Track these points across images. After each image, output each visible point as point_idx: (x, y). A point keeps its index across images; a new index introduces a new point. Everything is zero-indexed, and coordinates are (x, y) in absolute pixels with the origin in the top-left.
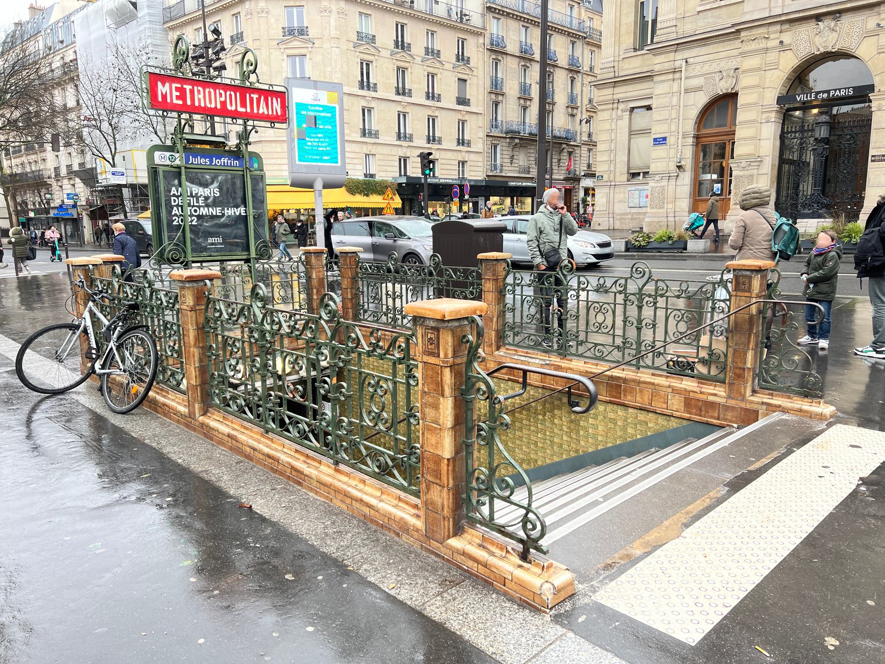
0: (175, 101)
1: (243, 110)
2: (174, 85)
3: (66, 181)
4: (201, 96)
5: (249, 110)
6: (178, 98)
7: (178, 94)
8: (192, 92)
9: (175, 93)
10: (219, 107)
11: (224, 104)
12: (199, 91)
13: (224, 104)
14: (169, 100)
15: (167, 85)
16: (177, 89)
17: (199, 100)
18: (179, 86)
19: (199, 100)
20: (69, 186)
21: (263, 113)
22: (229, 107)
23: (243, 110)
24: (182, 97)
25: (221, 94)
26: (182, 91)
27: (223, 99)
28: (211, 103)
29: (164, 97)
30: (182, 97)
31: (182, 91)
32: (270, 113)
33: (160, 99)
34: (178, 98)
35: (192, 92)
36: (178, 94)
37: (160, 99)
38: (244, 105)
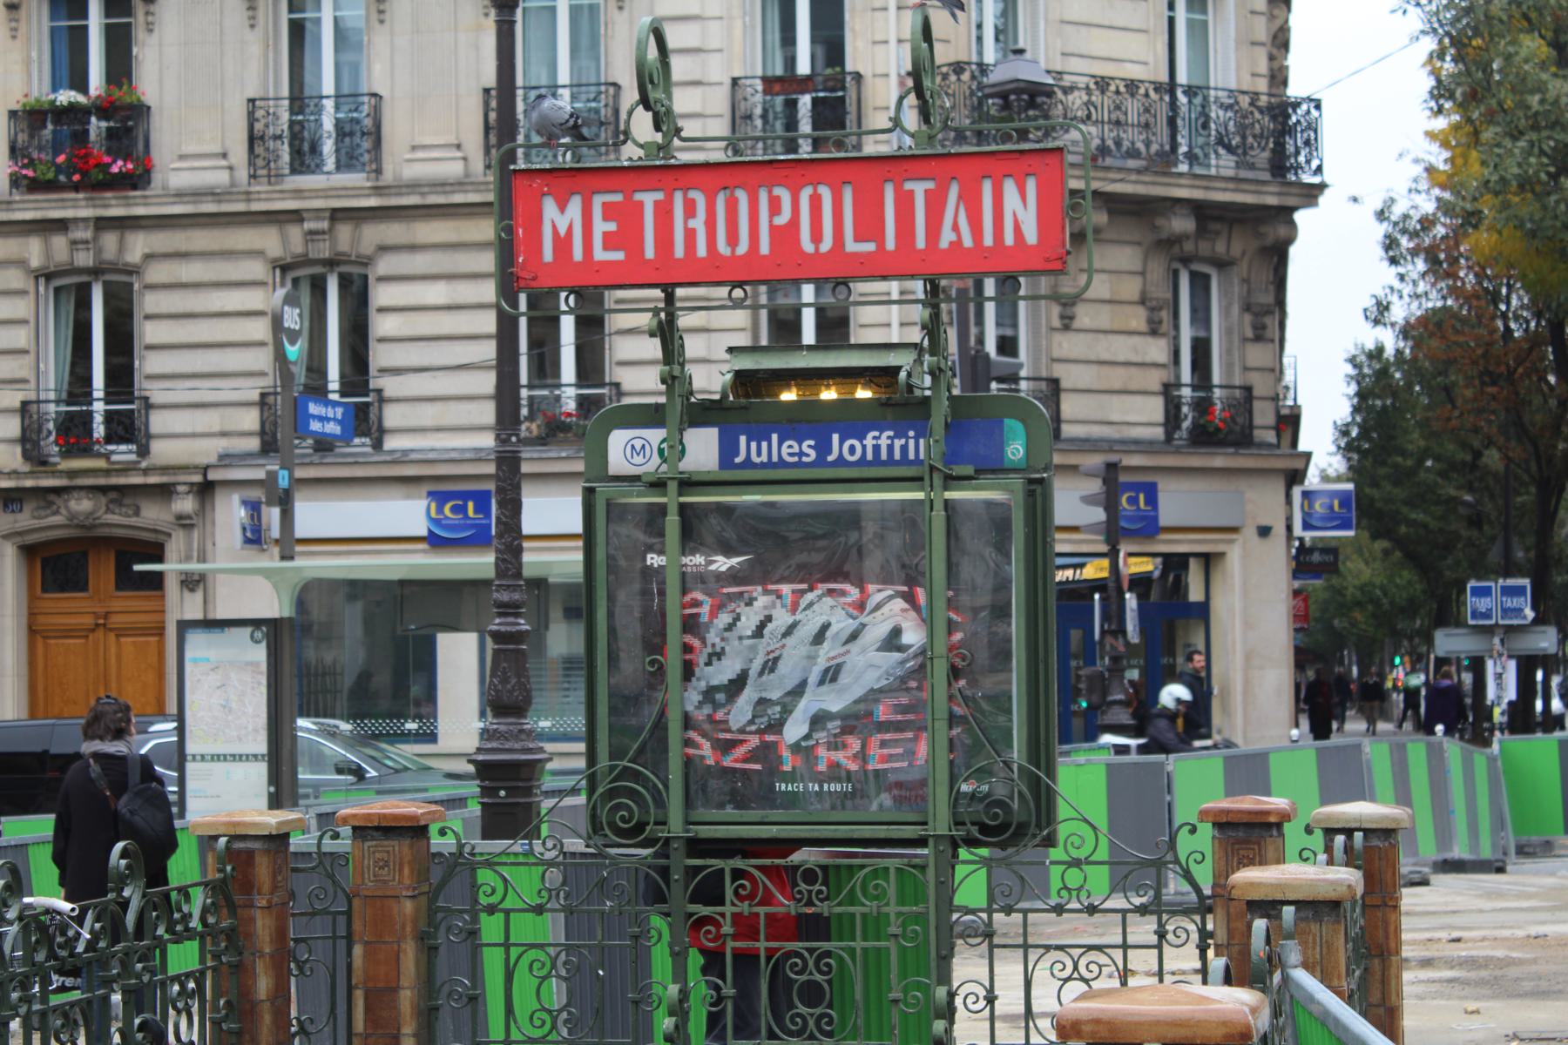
0: (600, 254)
1: (870, 247)
2: (598, 201)
4: (698, 223)
5: (890, 244)
6: (610, 242)
7: (612, 226)
8: (664, 213)
10: (765, 249)
11: (785, 236)
12: (690, 210)
13: (785, 236)
14: (578, 254)
15: (575, 205)
16: (609, 212)
17: (690, 235)
18: (618, 198)
19: (690, 235)
21: (957, 244)
22: (807, 246)
23: (870, 247)
24: (626, 237)
25: (775, 207)
26: (627, 217)
27: (783, 219)
28: (733, 240)
29: (563, 244)
30: (626, 237)
31: (627, 217)
32: (988, 241)
33: (548, 255)
34: (610, 242)
35: (664, 213)
36: (612, 226)
37: (548, 255)
38: (869, 226)
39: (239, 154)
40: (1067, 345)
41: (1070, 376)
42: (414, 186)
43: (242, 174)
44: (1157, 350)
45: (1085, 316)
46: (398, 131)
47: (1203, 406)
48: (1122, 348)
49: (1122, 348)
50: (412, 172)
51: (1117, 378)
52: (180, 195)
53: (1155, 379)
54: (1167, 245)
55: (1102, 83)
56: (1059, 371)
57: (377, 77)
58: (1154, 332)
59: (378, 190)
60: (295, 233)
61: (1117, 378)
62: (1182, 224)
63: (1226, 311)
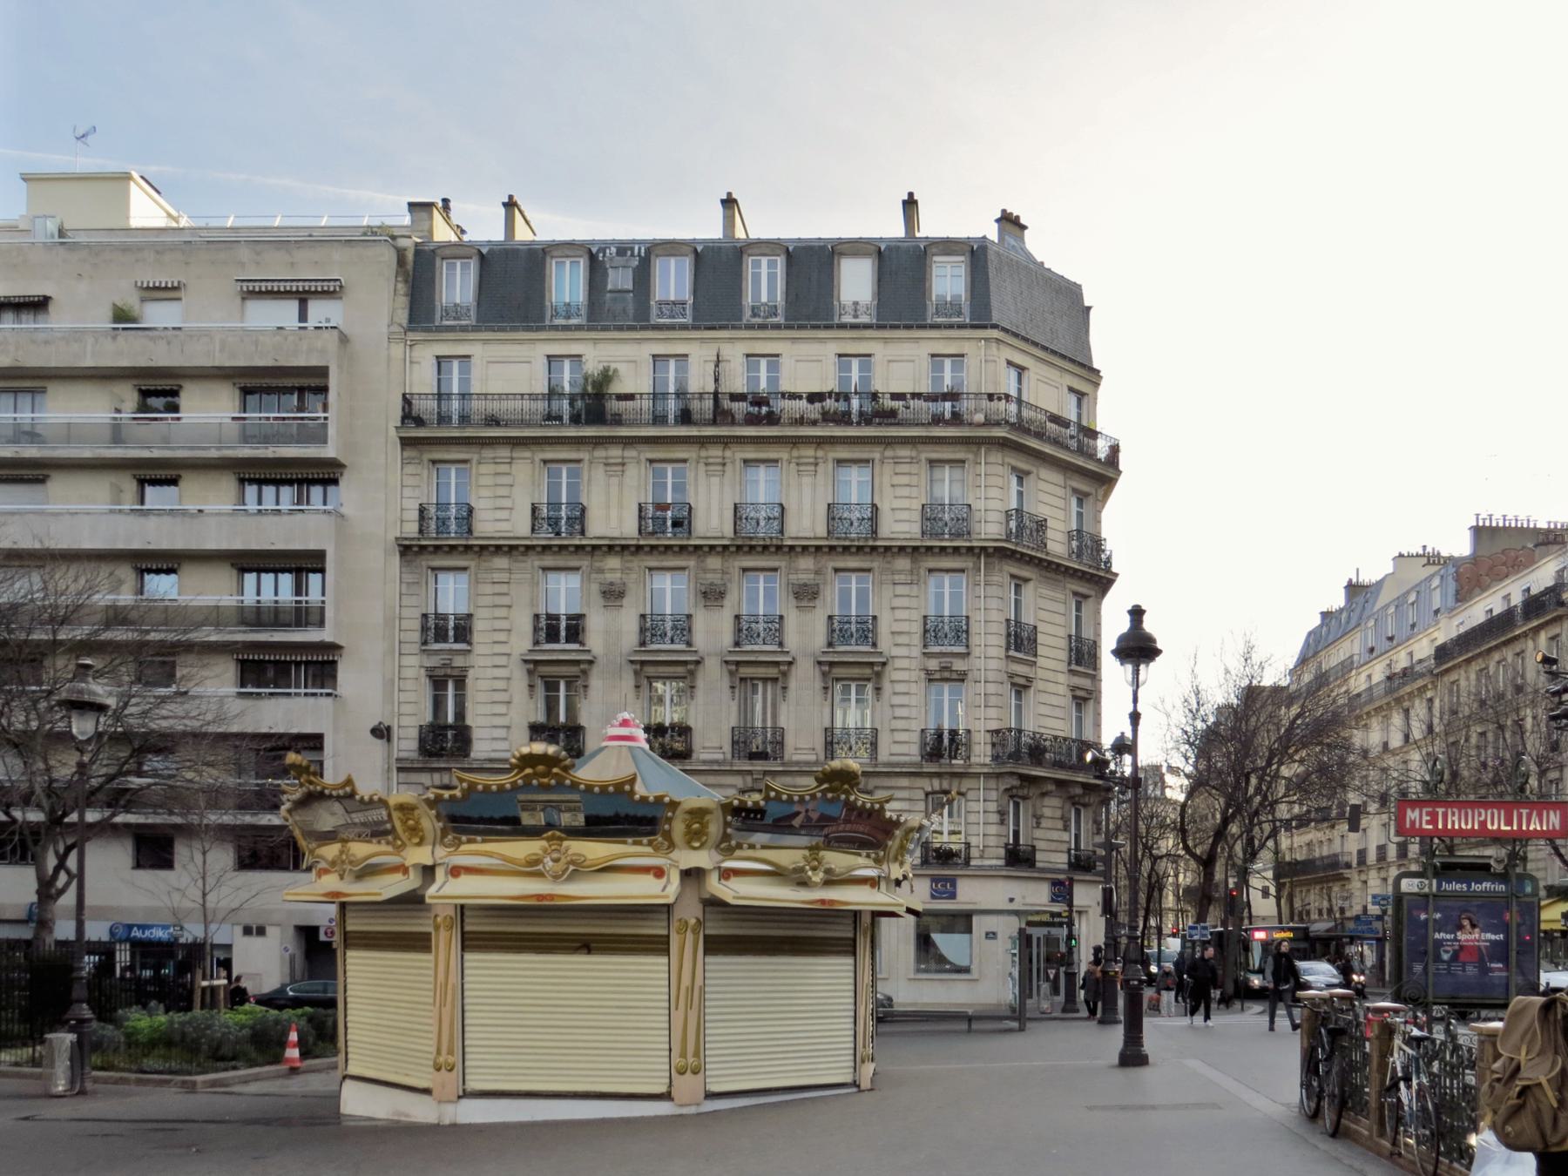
0: (1425, 826)
3: (1373, 873)
6: (1428, 823)
9: (1426, 818)
16: (1428, 814)
20: (1378, 882)
24: (1434, 821)
30: (1434, 821)
39: (727, 748)
40: (1038, 833)
41: (1040, 845)
42: (797, 763)
43: (729, 756)
44: (1065, 836)
45: (1044, 823)
46: (790, 741)
47: (1077, 857)
48: (1055, 835)
49: (1055, 835)
50: (795, 758)
51: (1053, 846)
52: (705, 762)
53: (1064, 847)
54: (1071, 798)
55: (1056, 738)
56: (1036, 843)
57: (782, 722)
58: (1066, 828)
59: (783, 764)
60: (749, 779)
61: (1053, 846)
62: (1079, 791)
63: (1026, 821)
